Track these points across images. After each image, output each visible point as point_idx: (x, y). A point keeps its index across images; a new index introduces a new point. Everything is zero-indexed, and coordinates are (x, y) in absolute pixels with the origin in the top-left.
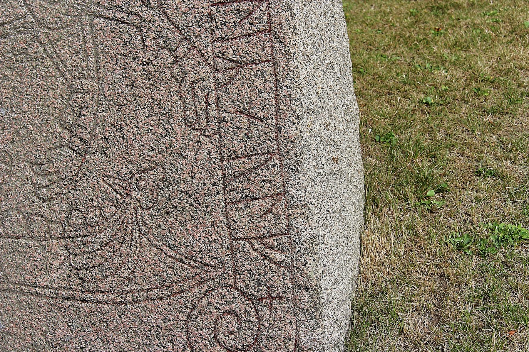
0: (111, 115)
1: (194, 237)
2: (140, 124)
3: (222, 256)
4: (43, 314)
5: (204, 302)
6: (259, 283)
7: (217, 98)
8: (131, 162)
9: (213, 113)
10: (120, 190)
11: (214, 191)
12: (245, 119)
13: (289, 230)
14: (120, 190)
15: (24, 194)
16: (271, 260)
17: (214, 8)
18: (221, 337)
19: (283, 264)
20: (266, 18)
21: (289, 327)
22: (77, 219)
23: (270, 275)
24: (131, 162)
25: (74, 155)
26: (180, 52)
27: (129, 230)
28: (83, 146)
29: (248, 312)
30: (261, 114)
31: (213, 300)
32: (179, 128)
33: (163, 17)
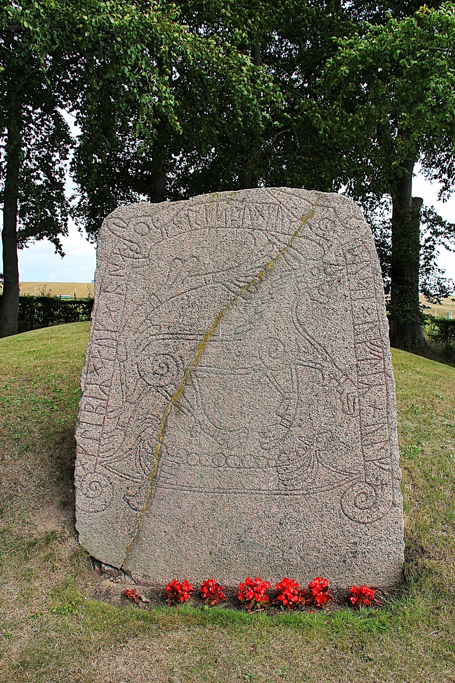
0: (305, 408)
1: (347, 461)
2: (320, 413)
3: (360, 469)
4: (263, 503)
5: (350, 490)
6: (377, 479)
7: (359, 400)
8: (314, 430)
9: (357, 407)
10: (308, 443)
11: (357, 441)
12: (372, 409)
13: (391, 455)
14: (308, 443)
15: (254, 447)
16: (383, 469)
17: (359, 362)
18: (358, 504)
19: (388, 470)
20: (383, 367)
21: (390, 496)
22: (284, 457)
23: (382, 475)
24: (314, 430)
25: (283, 428)
26: (342, 381)
27: (312, 461)
28: (288, 424)
29: (371, 492)
30: (380, 407)
31: (355, 488)
32: (340, 414)
33: (333, 365)
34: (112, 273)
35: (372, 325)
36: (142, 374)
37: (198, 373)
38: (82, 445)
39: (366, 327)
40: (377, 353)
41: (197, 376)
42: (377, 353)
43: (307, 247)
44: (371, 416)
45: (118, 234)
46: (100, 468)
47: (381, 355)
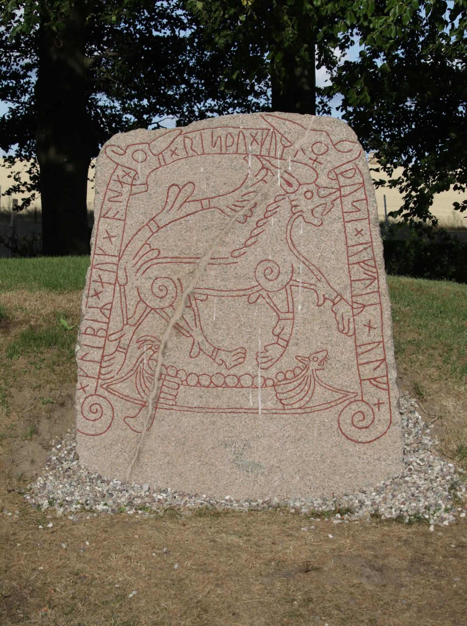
7: (354, 320)
9: (351, 326)
26: (336, 301)
32: (336, 333)
34: (112, 199)
35: (365, 246)
36: (142, 296)
37: (196, 296)
38: (83, 368)
39: (361, 248)
40: (371, 274)
41: (195, 299)
42: (371, 274)
43: (301, 170)
44: (366, 334)
45: (116, 161)
46: (101, 391)
47: (375, 275)
